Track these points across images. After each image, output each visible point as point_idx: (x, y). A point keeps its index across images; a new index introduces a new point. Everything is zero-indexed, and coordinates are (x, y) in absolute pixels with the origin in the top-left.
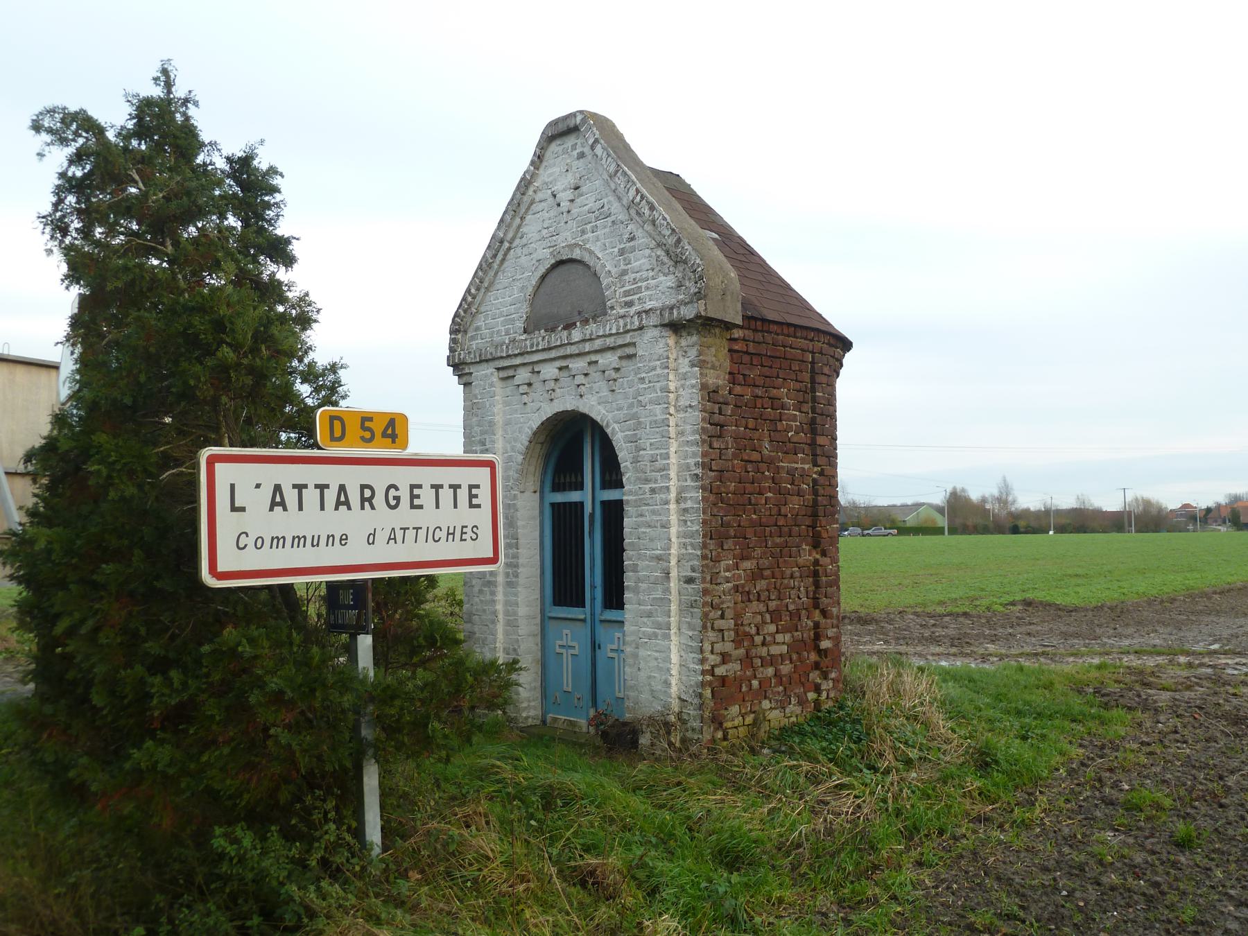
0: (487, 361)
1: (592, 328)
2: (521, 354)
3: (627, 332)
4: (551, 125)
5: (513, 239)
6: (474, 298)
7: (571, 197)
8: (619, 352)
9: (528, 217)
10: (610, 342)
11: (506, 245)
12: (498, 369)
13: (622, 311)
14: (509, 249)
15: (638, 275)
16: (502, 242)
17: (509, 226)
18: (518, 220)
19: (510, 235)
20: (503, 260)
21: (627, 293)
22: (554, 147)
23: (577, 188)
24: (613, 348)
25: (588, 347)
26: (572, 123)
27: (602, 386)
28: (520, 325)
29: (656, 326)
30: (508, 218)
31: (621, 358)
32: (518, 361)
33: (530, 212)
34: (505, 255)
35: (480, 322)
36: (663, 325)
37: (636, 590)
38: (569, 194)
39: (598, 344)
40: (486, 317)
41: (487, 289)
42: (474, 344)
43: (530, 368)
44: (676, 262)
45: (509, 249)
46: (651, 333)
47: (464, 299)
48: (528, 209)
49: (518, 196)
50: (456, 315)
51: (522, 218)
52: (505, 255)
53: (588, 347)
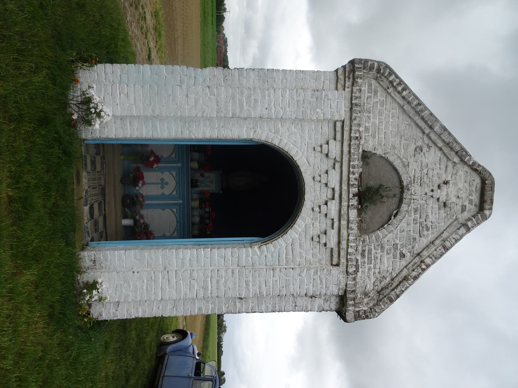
0: (351, 109)
1: (354, 226)
2: (350, 152)
3: (347, 261)
4: (493, 183)
5: (430, 138)
6: (399, 92)
7: (441, 200)
8: (336, 250)
9: (439, 153)
10: (344, 243)
11: (427, 131)
12: (343, 122)
13: (360, 248)
14: (424, 133)
15: (379, 261)
16: (431, 127)
17: (439, 136)
18: (440, 144)
19: (433, 136)
20: (417, 125)
21: (370, 252)
22: (478, 181)
23: (445, 205)
24: (339, 243)
25: (344, 223)
26: (487, 206)
27: (314, 231)
28: (369, 147)
29: (346, 285)
30: (445, 137)
31: (332, 249)
32: (346, 149)
33: (443, 156)
34: (420, 128)
35: (381, 96)
36: (345, 291)
37: (196, 135)
38: (443, 199)
39: (344, 232)
40: (382, 104)
41: (402, 107)
42: (365, 88)
43: (338, 159)
44: (378, 292)
45: (424, 133)
46: (342, 277)
47: (401, 82)
48: (445, 155)
49: (457, 148)
50: (392, 72)
51: (440, 149)
52: (420, 128)
53: (344, 223)
